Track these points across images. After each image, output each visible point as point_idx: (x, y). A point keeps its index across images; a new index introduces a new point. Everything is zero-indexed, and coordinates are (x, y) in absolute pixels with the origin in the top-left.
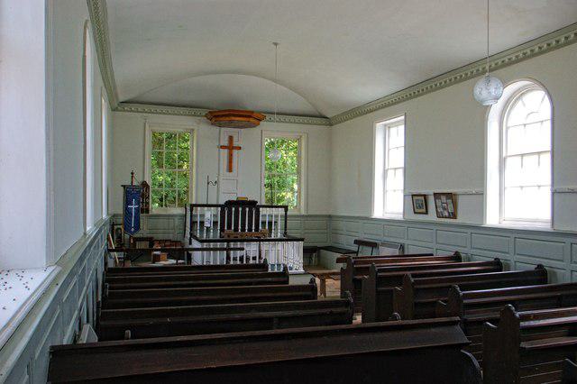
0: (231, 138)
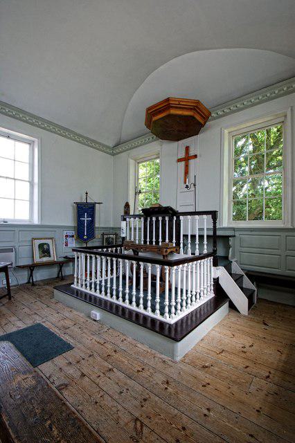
0: (187, 148)
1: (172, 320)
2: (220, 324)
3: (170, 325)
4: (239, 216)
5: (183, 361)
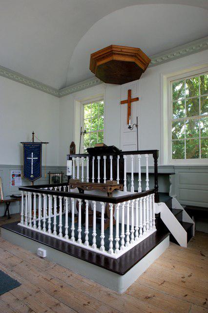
0: (130, 91)
1: (116, 254)
2: (162, 257)
3: (115, 260)
4: (178, 155)
5: (127, 293)
